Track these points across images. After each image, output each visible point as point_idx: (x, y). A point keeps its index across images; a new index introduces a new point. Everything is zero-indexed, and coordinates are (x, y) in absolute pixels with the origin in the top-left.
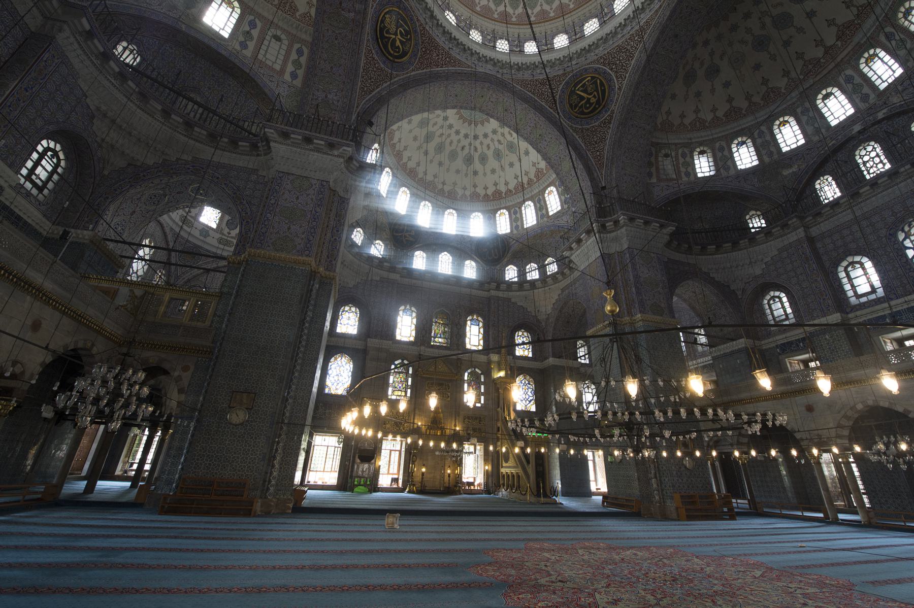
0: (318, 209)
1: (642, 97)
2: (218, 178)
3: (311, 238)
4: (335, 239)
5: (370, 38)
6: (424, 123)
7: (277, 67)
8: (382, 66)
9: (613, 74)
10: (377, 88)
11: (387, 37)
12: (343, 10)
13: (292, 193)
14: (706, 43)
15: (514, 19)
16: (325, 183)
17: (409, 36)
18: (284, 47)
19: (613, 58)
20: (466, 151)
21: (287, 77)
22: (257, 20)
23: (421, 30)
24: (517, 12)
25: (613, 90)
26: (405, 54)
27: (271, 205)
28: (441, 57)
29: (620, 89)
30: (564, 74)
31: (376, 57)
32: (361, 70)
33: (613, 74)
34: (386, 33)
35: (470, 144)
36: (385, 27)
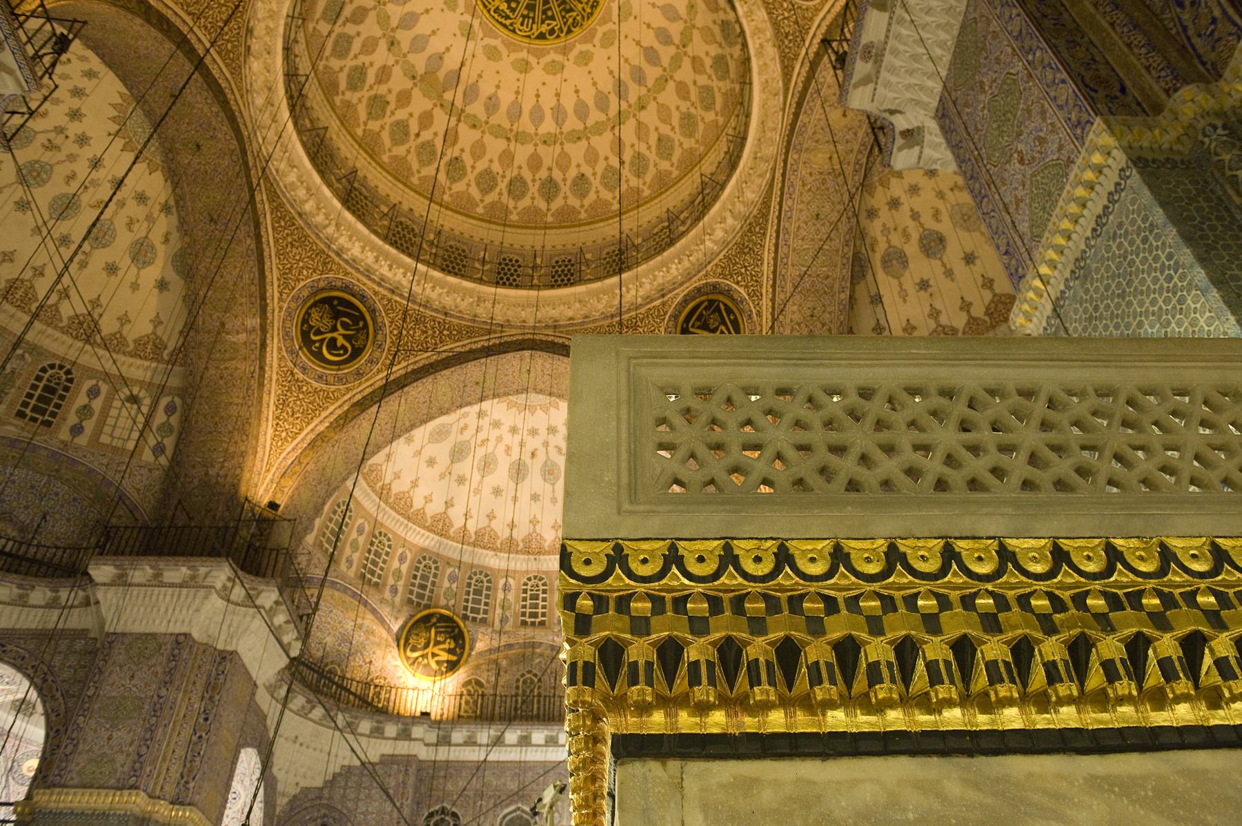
0: (163, 692)
1: (799, 324)
2: (23, 658)
3: (144, 750)
4: (200, 737)
5: (284, 353)
6: (440, 435)
7: (131, 445)
8: (315, 384)
9: (741, 290)
10: (308, 424)
11: (315, 342)
12: (228, 333)
13: (125, 668)
14: (894, 204)
15: (583, 215)
16: (182, 639)
17: (361, 324)
18: (145, 410)
19: (734, 264)
20: (541, 457)
21: (147, 456)
22: (100, 383)
23: (384, 306)
24: (587, 202)
25: (750, 317)
26: (357, 352)
27: (87, 699)
28: (430, 332)
29: (759, 314)
30: (664, 304)
31: (301, 376)
32: (272, 407)
33: (741, 290)
34: (315, 334)
35: (546, 444)
36: (311, 327)
